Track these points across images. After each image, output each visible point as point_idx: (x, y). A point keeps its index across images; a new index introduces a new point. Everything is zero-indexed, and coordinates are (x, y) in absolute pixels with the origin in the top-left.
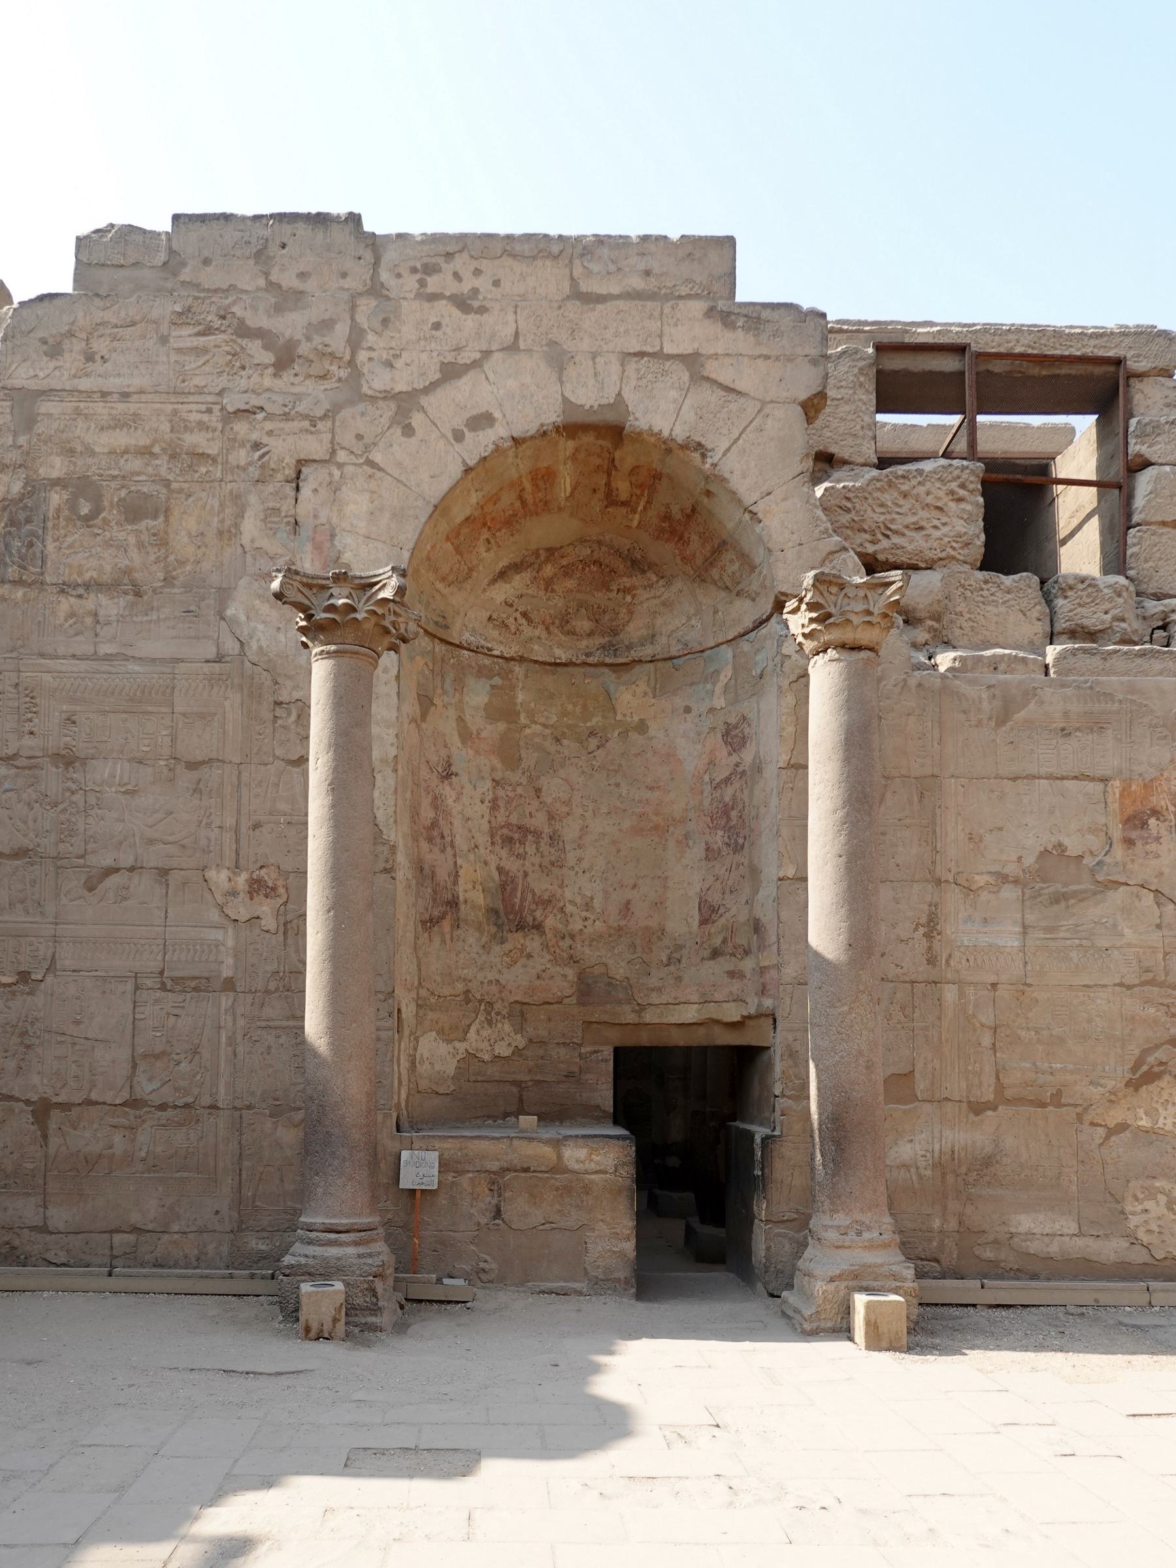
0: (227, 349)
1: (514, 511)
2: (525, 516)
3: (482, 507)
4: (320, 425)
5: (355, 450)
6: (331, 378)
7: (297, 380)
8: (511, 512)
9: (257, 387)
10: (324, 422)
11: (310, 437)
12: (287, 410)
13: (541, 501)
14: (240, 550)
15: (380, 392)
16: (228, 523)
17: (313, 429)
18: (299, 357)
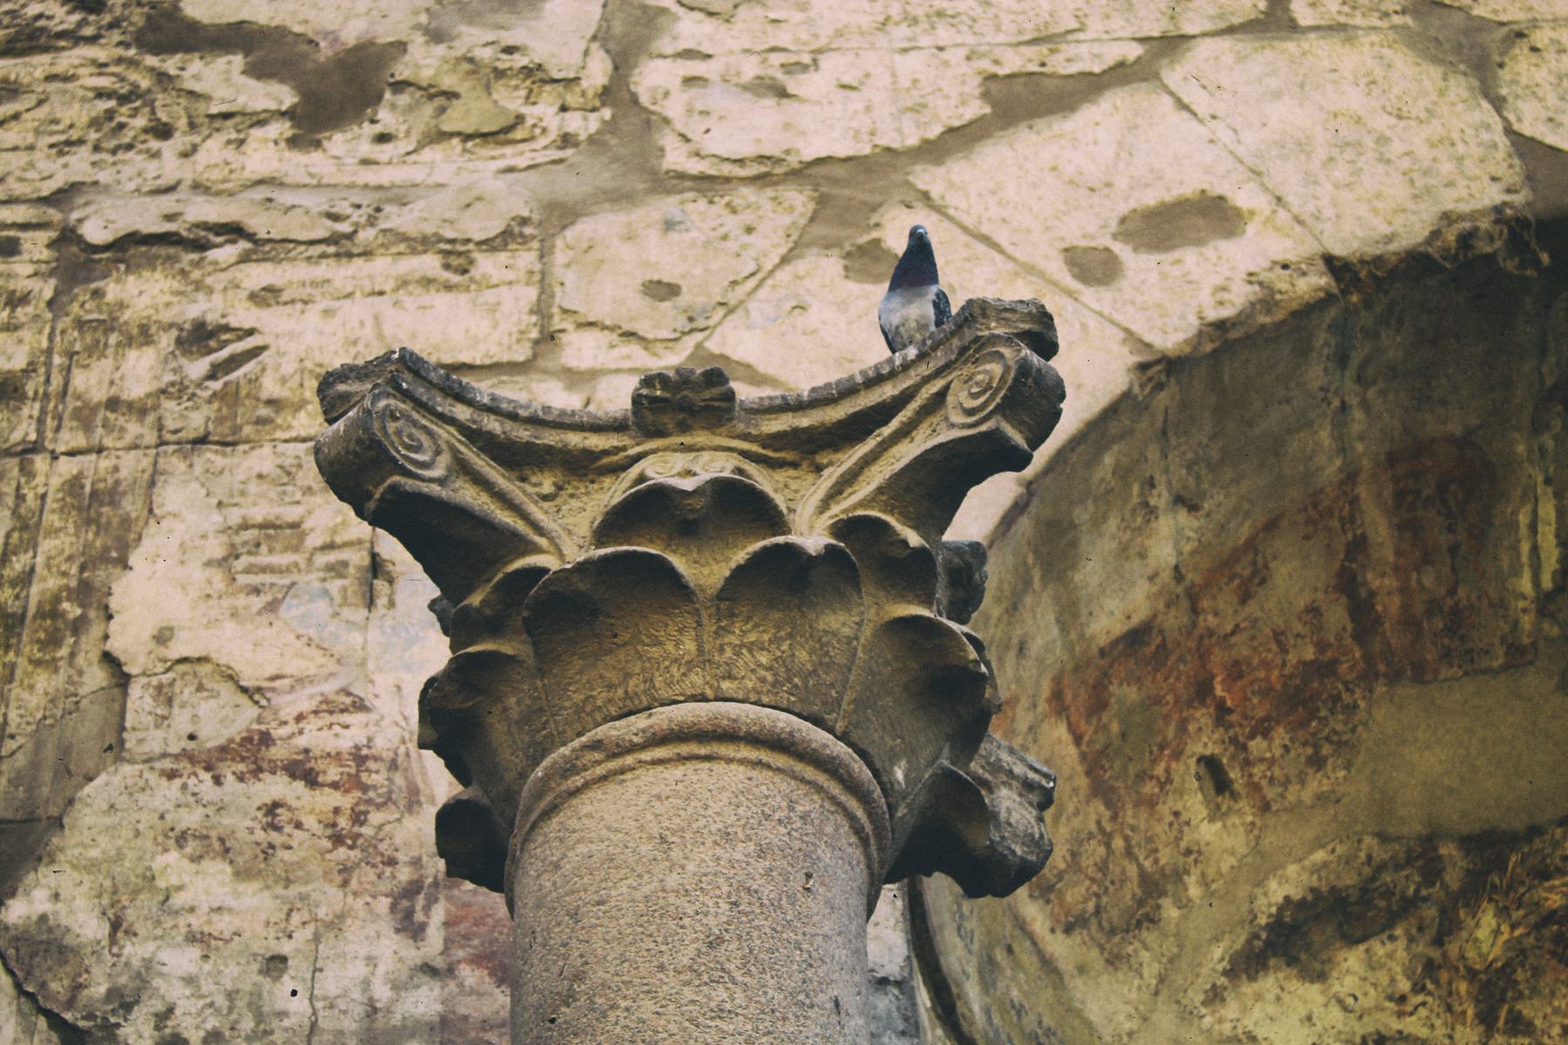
0: (104, 82)
1: (1321, 646)
2: (1368, 676)
3: (1193, 597)
4: (487, 265)
5: (643, 328)
6: (532, 138)
7: (385, 152)
8: (1309, 653)
9: (215, 175)
10: (503, 257)
11: (440, 300)
12: (345, 227)
13: (1433, 607)
14: (96, 677)
15: (740, 162)
16: (44, 585)
17: (455, 278)
18: (400, 86)
